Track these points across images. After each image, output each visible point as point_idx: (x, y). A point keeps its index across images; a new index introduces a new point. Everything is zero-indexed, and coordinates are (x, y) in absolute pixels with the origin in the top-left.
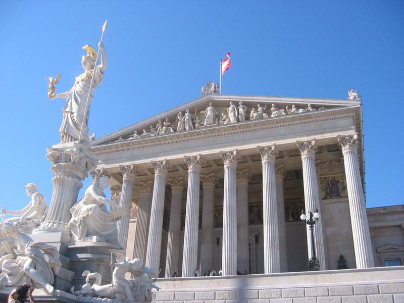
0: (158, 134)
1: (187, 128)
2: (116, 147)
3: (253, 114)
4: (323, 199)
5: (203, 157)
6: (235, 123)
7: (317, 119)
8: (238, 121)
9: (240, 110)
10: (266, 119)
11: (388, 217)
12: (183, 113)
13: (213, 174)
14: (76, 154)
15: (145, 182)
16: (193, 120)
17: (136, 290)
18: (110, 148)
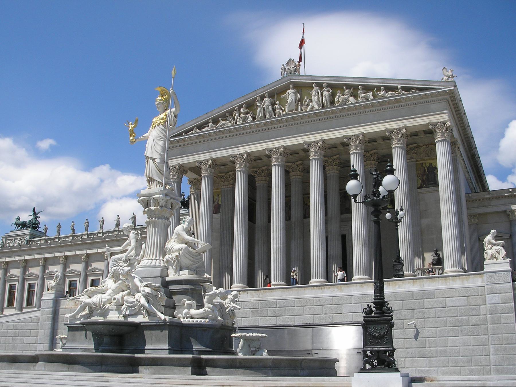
0: (236, 123)
1: (267, 115)
2: (190, 138)
3: (339, 98)
4: (418, 188)
5: (286, 147)
6: (319, 110)
7: (409, 102)
8: (323, 106)
9: (325, 93)
10: (352, 104)
11: (493, 203)
12: (262, 97)
13: (300, 162)
14: (162, 200)
15: (226, 173)
16: (273, 105)
17: (223, 311)
18: (183, 140)
